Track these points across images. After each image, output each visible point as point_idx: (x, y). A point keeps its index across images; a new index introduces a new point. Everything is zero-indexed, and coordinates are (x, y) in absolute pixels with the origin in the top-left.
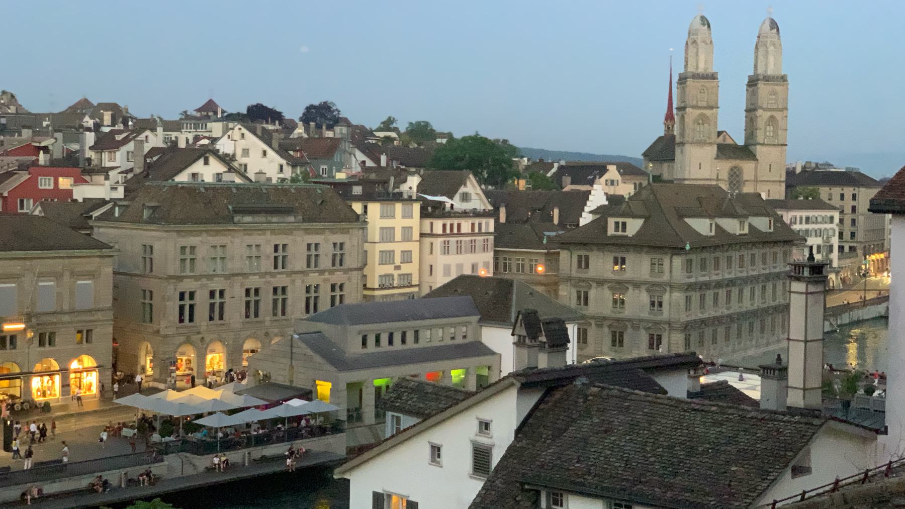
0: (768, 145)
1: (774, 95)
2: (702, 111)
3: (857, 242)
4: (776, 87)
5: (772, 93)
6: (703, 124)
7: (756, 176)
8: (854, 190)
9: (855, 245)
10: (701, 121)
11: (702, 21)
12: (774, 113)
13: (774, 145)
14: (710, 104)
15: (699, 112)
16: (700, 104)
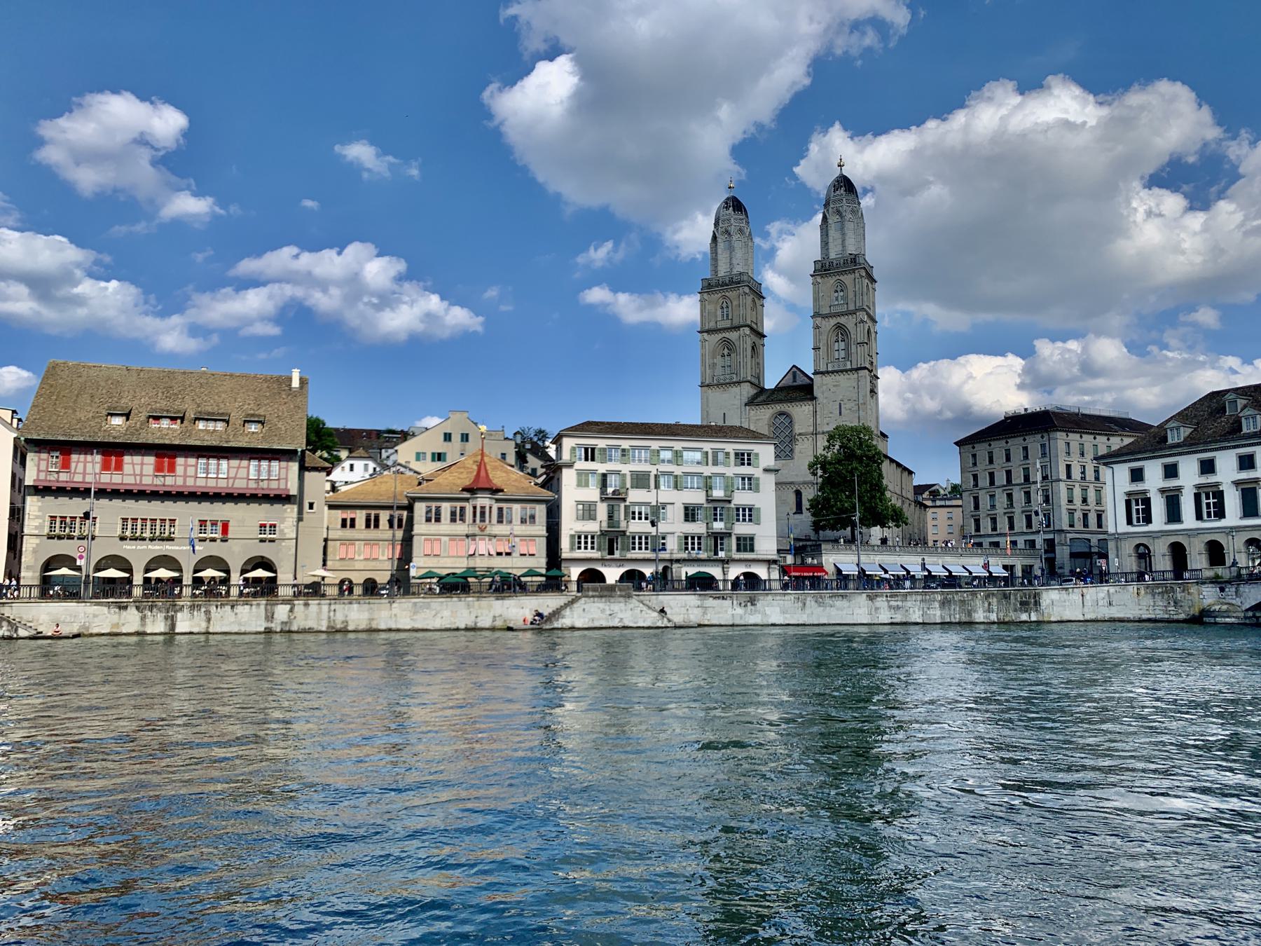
0: (833, 372)
1: (842, 291)
2: (724, 335)
3: (1054, 532)
4: (841, 278)
5: (839, 289)
6: (729, 355)
7: (815, 425)
8: (1042, 437)
9: (1051, 536)
10: (726, 351)
11: (726, 203)
12: (842, 320)
13: (846, 371)
14: (736, 323)
15: (720, 336)
16: (721, 325)
